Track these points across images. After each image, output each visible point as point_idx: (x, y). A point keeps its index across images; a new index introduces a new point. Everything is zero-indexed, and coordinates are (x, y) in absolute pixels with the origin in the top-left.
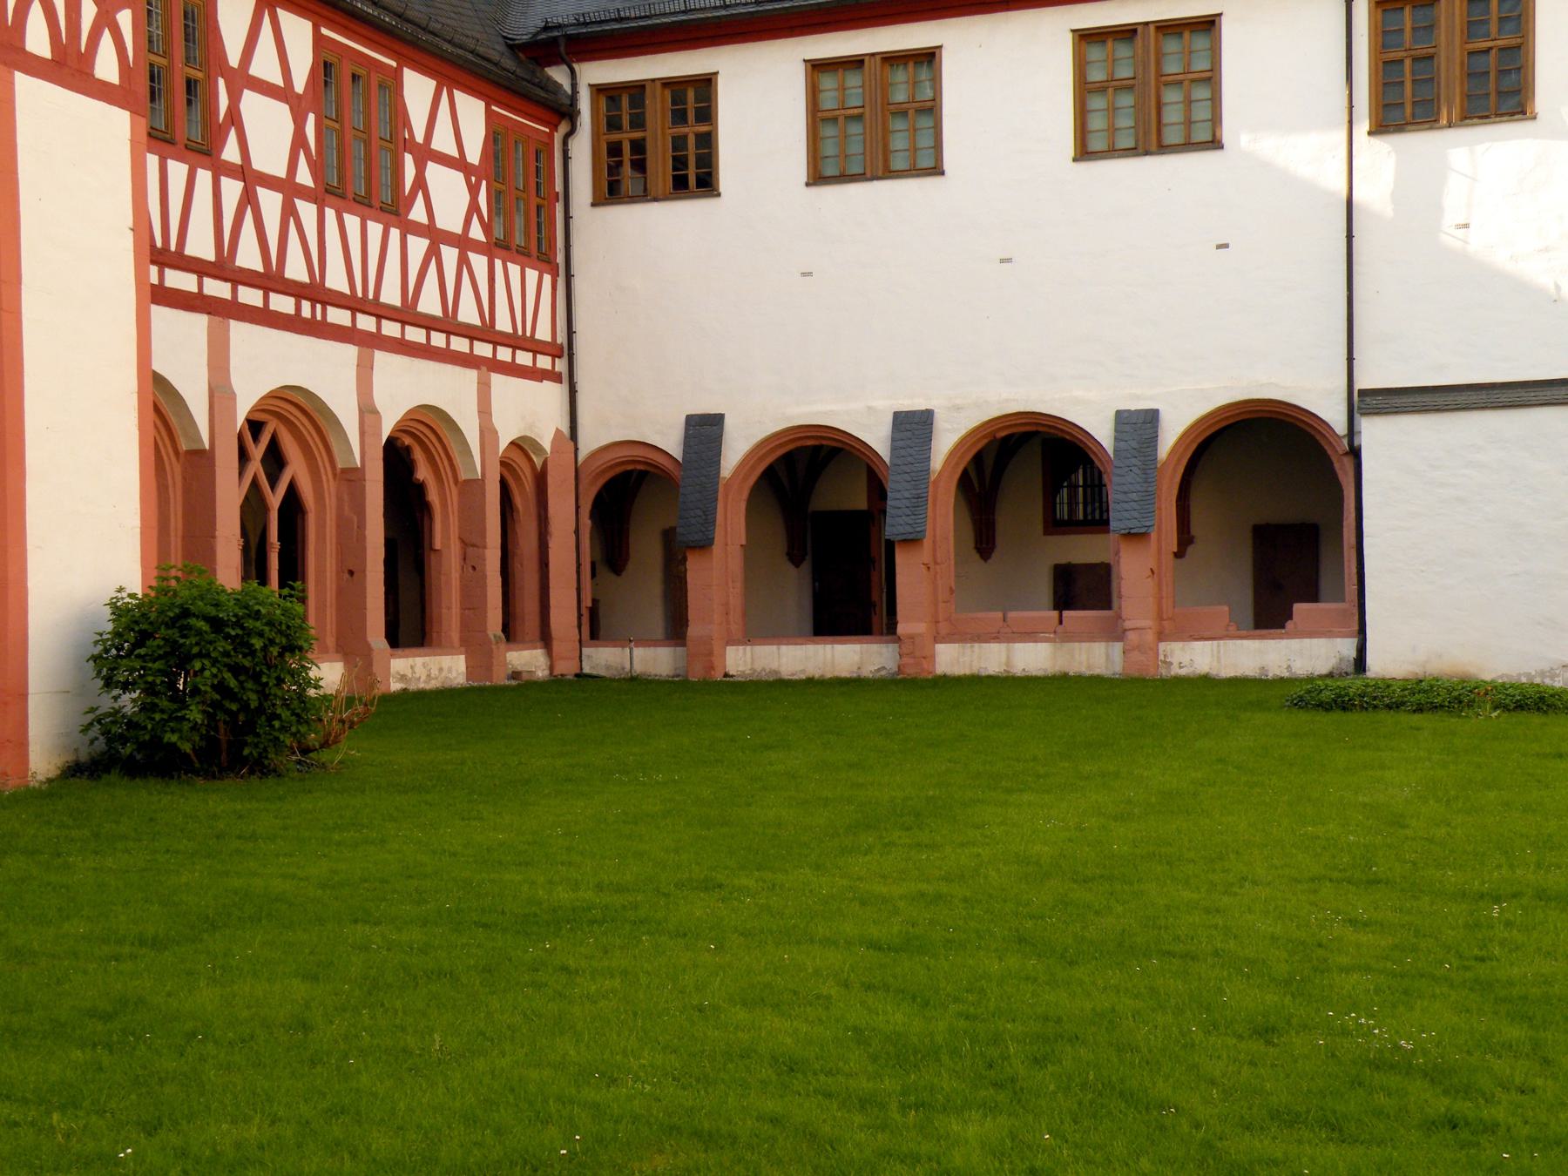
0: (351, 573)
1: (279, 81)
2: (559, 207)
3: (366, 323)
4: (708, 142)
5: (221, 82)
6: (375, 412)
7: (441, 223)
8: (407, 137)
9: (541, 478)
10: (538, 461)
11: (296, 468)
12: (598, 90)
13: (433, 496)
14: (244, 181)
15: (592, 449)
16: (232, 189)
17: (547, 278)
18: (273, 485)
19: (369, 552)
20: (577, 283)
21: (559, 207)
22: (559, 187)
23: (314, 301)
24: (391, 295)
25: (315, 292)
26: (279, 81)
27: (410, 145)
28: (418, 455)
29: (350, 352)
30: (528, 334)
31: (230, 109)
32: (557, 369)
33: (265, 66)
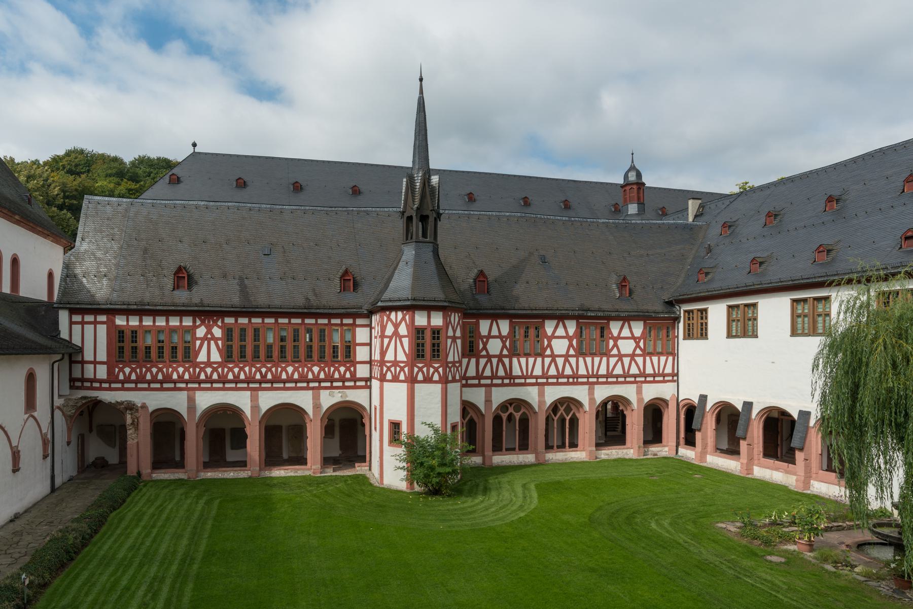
2: (676, 339)
4: (706, 324)
5: (545, 340)
7: (623, 352)
12: (685, 311)
16: (547, 360)
17: (670, 358)
21: (676, 339)
23: (573, 378)
25: (575, 376)
28: (620, 404)
29: (587, 387)
30: (661, 372)
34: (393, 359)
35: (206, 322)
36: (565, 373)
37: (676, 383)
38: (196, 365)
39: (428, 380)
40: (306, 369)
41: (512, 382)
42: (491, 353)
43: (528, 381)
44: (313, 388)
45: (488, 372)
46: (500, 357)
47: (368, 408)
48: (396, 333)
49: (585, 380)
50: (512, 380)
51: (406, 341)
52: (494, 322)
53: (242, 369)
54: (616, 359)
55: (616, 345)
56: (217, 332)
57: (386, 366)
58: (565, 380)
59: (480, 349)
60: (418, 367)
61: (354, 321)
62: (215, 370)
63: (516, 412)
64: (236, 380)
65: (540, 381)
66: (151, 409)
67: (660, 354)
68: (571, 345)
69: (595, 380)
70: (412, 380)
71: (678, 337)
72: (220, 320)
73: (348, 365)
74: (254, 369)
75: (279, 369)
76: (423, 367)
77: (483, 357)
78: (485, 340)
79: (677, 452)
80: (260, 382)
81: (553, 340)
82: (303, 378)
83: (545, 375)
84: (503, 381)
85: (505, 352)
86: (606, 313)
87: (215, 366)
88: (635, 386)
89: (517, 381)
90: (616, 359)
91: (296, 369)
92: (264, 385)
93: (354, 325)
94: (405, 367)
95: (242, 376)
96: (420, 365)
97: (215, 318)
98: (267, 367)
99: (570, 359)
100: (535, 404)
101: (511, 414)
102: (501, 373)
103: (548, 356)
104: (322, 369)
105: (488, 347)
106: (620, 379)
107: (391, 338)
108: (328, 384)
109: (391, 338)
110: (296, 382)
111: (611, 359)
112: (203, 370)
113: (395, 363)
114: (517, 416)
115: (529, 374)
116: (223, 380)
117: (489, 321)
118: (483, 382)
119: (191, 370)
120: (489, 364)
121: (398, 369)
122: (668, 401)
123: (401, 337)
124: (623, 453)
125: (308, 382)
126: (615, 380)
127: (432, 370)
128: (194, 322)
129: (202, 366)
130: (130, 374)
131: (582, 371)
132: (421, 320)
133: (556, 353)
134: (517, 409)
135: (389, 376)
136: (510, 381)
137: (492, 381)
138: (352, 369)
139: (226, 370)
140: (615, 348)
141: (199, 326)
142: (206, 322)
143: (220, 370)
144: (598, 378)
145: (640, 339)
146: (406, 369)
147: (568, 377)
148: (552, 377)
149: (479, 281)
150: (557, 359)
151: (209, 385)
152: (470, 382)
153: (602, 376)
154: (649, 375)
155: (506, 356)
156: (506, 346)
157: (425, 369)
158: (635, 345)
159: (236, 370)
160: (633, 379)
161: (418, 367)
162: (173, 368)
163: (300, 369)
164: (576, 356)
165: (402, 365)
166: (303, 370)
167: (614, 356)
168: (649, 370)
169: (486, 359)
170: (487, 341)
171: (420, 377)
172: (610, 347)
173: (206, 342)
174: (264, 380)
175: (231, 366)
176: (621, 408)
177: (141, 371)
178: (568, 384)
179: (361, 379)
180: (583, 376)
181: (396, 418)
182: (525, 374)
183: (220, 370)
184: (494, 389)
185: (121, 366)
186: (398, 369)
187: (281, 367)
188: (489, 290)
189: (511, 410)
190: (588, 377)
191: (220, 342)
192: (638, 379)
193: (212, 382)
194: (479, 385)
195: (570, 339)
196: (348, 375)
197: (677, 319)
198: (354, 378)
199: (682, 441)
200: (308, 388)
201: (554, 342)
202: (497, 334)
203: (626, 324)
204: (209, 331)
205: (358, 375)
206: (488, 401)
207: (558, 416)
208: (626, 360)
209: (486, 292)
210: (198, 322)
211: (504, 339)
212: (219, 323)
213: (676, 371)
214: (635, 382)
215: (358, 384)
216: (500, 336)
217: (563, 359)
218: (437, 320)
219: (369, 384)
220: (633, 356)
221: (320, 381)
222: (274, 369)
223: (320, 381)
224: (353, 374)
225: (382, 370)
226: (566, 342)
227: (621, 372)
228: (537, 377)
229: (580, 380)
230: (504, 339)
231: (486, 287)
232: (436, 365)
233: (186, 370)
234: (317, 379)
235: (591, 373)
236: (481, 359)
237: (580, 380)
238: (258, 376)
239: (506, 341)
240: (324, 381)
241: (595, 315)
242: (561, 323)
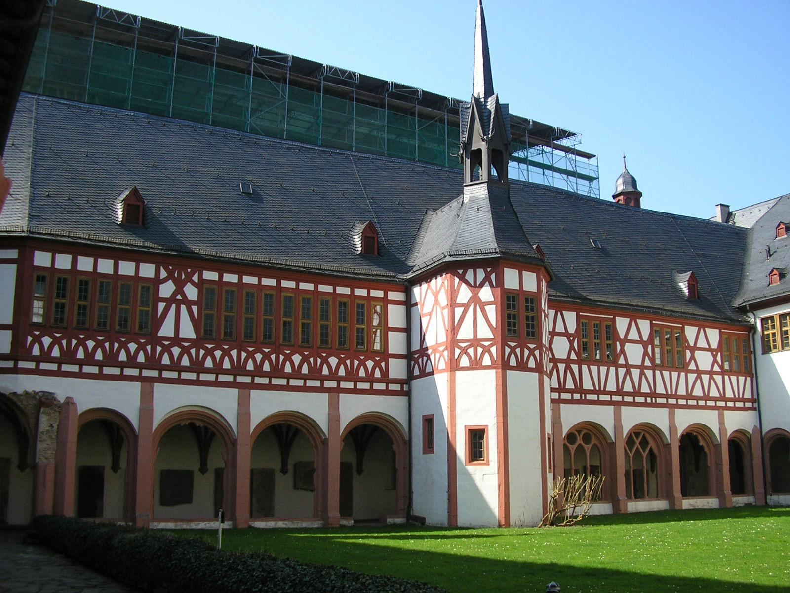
0: (669, 474)
2: (753, 355)
3: (672, 401)
5: (618, 343)
9: (750, 441)
10: (749, 436)
11: (652, 444)
13: (706, 449)
14: (626, 368)
15: (768, 430)
16: (622, 371)
17: (749, 379)
18: (644, 451)
19: (674, 467)
20: (760, 379)
21: (753, 355)
22: (752, 350)
24: (682, 391)
25: (653, 394)
27: (689, 348)
28: (700, 438)
29: (666, 410)
30: (741, 397)
31: (621, 349)
32: (755, 406)
33: (633, 335)
34: (471, 336)
35: (176, 275)
37: (758, 411)
38: (156, 341)
39: (522, 366)
40: (319, 360)
43: (603, 398)
44: (329, 390)
46: (568, 362)
47: (405, 424)
48: (475, 300)
49: (663, 401)
51: (491, 311)
53: (226, 353)
55: (693, 357)
56: (191, 292)
57: (460, 348)
60: (509, 347)
62: (185, 351)
63: (587, 443)
64: (218, 369)
66: (81, 409)
67: (738, 373)
70: (504, 366)
72: (197, 273)
73: (378, 359)
74: (244, 355)
75: (282, 357)
76: (516, 347)
80: (253, 374)
82: (315, 373)
83: (619, 392)
85: (573, 356)
87: (186, 344)
88: (716, 412)
91: (305, 359)
92: (259, 380)
93: (385, 301)
94: (491, 345)
95: (227, 365)
96: (513, 344)
97: (189, 270)
98: (263, 353)
102: (570, 385)
103: (622, 366)
104: (341, 362)
107: (466, 307)
108: (350, 385)
109: (466, 307)
110: (305, 378)
112: (167, 349)
113: (475, 342)
116: (197, 366)
119: (149, 348)
121: (480, 350)
123: (483, 305)
125: (323, 379)
127: (526, 352)
128: (157, 272)
129: (166, 343)
130: (51, 347)
131: (660, 390)
132: (511, 278)
135: (465, 362)
138: (383, 364)
139: (202, 352)
140: (693, 361)
141: (165, 280)
142: (176, 275)
143: (193, 351)
144: (677, 399)
145: (716, 351)
146: (493, 350)
147: (645, 395)
148: (628, 394)
151: (174, 375)
153: (682, 397)
155: (574, 362)
156: (575, 349)
157: (518, 351)
159: (218, 354)
161: (509, 347)
162: (120, 342)
163: (311, 360)
165: (486, 344)
166: (315, 362)
167: (692, 371)
171: (513, 362)
172: (687, 361)
173: (174, 306)
174: (258, 371)
175: (210, 346)
177: (69, 344)
178: (645, 405)
179: (395, 381)
180: (661, 396)
181: (476, 422)
183: (193, 351)
185: (37, 333)
186: (480, 350)
187: (285, 354)
189: (579, 441)
190: (667, 396)
191: (195, 309)
193: (181, 369)
196: (377, 374)
198: (385, 378)
199: (769, 490)
200: (321, 390)
201: (628, 347)
204: (179, 290)
205: (392, 375)
207: (634, 451)
208: (705, 378)
210: (163, 274)
212: (195, 278)
213: (755, 397)
214: (715, 408)
215: (392, 387)
216: (566, 334)
218: (530, 281)
219: (406, 388)
220: (711, 373)
221: (339, 380)
222: (273, 357)
223: (339, 380)
224: (385, 373)
225: (452, 353)
226: (640, 348)
228: (611, 393)
229: (659, 401)
230: (571, 338)
232: (532, 346)
233: (141, 347)
234: (333, 375)
237: (659, 401)
238: (250, 366)
240: (345, 379)
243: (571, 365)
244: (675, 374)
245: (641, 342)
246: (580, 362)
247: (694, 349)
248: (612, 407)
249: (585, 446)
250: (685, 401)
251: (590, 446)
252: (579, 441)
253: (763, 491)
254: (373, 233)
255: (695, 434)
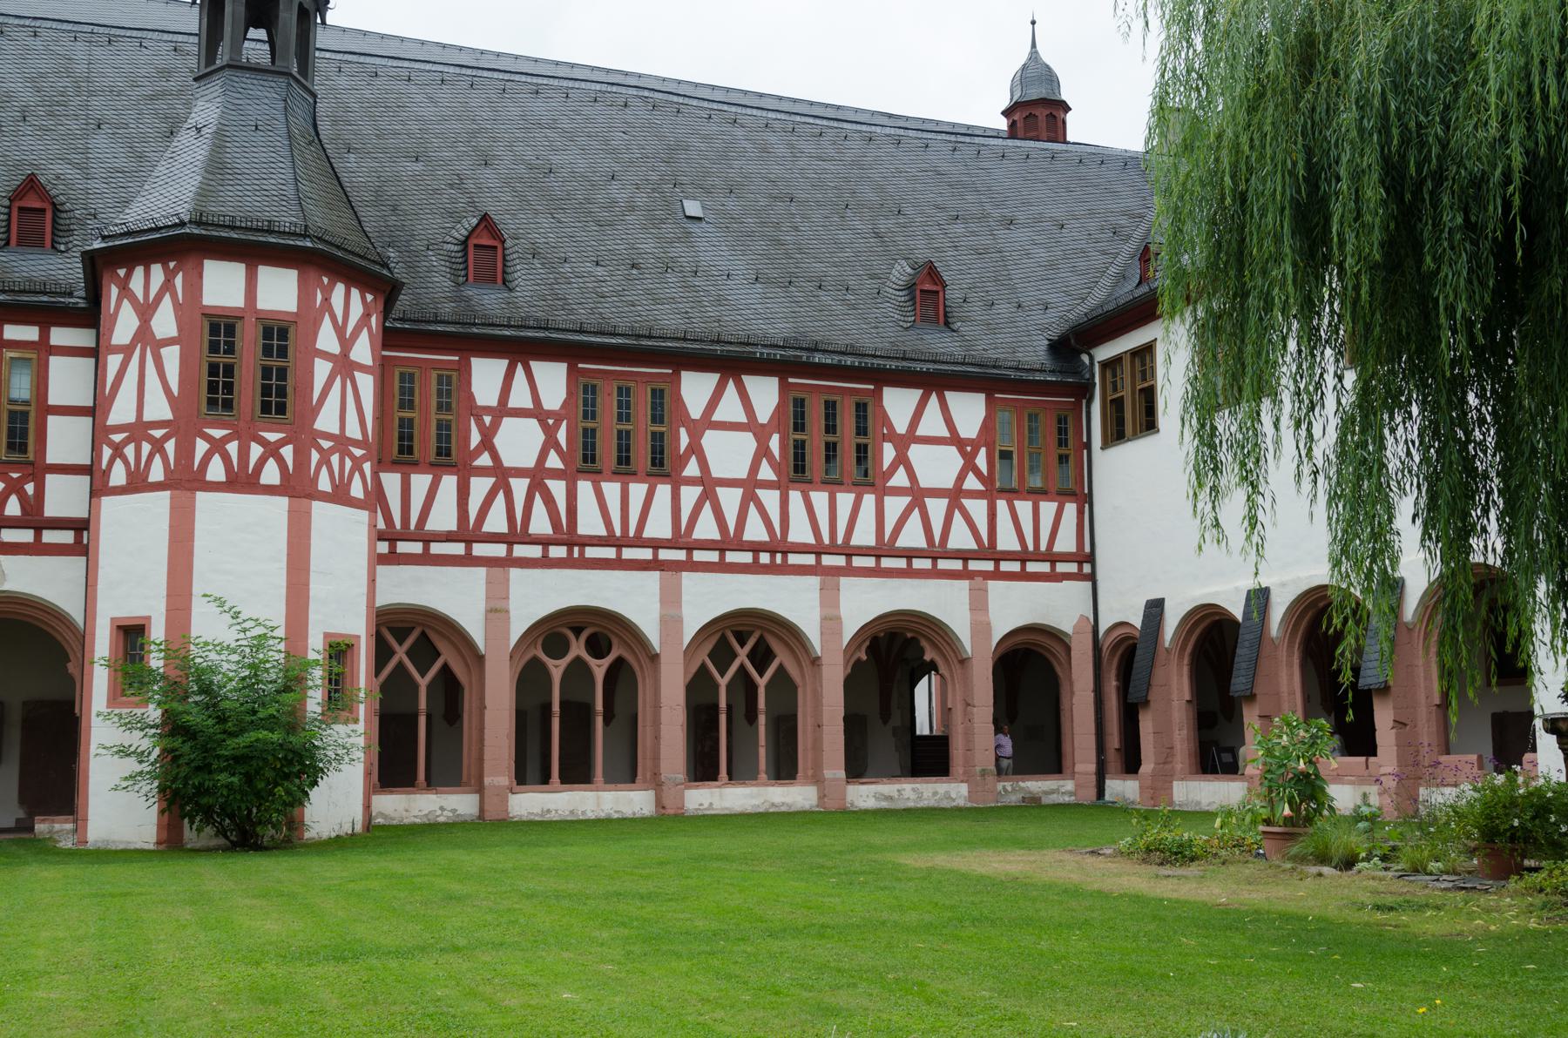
1: (743, 418)
2: (1085, 452)
5: (683, 431)
6: (838, 619)
7: (924, 482)
8: (885, 431)
11: (782, 657)
12: (1105, 365)
16: (690, 495)
17: (1071, 509)
21: (1085, 452)
23: (773, 553)
25: (779, 546)
26: (743, 418)
27: (892, 437)
28: (924, 643)
30: (1043, 547)
31: (690, 444)
36: (747, 536)
41: (576, 555)
42: (508, 462)
43: (628, 553)
45: (496, 522)
46: (538, 477)
49: (810, 560)
50: (576, 549)
52: (520, 369)
54: (906, 500)
55: (902, 460)
58: (746, 557)
59: (472, 447)
61: (45, 335)
65: (664, 555)
67: (1037, 495)
68: (762, 452)
69: (840, 561)
71: (1088, 446)
77: (483, 472)
78: (487, 419)
79: (1101, 792)
81: (708, 432)
84: (545, 551)
86: (869, 361)
88: (965, 584)
89: (592, 552)
90: (906, 500)
99: (762, 494)
100: (651, 629)
101: (578, 660)
102: (540, 524)
103: (691, 481)
105: (499, 441)
106: (919, 564)
111: (889, 501)
114: (599, 668)
115: (631, 534)
117: (501, 365)
118: (480, 550)
120: (501, 496)
122: (1066, 634)
124: (935, 794)
126: (901, 563)
133: (717, 472)
134: (597, 647)
136: (570, 552)
137: (510, 551)
144: (849, 556)
145: (976, 445)
147: (756, 548)
149: (476, 246)
150: (722, 492)
152: (437, 548)
153: (863, 552)
154: (1009, 556)
155: (556, 474)
158: (960, 462)
160: (957, 565)
164: (782, 486)
168: (1007, 540)
169: (493, 480)
170: (496, 425)
176: (927, 657)
178: (754, 568)
180: (802, 549)
182: (618, 533)
184: (515, 573)
188: (509, 277)
190: (818, 551)
192: (974, 565)
194: (468, 560)
195: (761, 434)
197: (1083, 391)
201: (711, 441)
202: (529, 404)
203: (934, 399)
206: (497, 612)
208: (937, 508)
209: (499, 281)
211: (551, 422)
213: (1087, 549)
216: (537, 412)
217: (739, 492)
220: (955, 496)
226: (748, 442)
227: (920, 542)
228: (656, 545)
229: (794, 559)
230: (551, 422)
231: (500, 265)
235: (826, 540)
236: (473, 480)
237: (794, 559)
239: (557, 426)
241: (835, 362)
242: (731, 385)
243: (546, 481)
244: (845, 500)
245: (751, 425)
246: (570, 476)
247: (903, 443)
248: (656, 574)
249: (592, 662)
250: (650, 550)
251: (564, 663)
252: (578, 649)
253: (1092, 767)
254: (43, 201)
255: (909, 635)
